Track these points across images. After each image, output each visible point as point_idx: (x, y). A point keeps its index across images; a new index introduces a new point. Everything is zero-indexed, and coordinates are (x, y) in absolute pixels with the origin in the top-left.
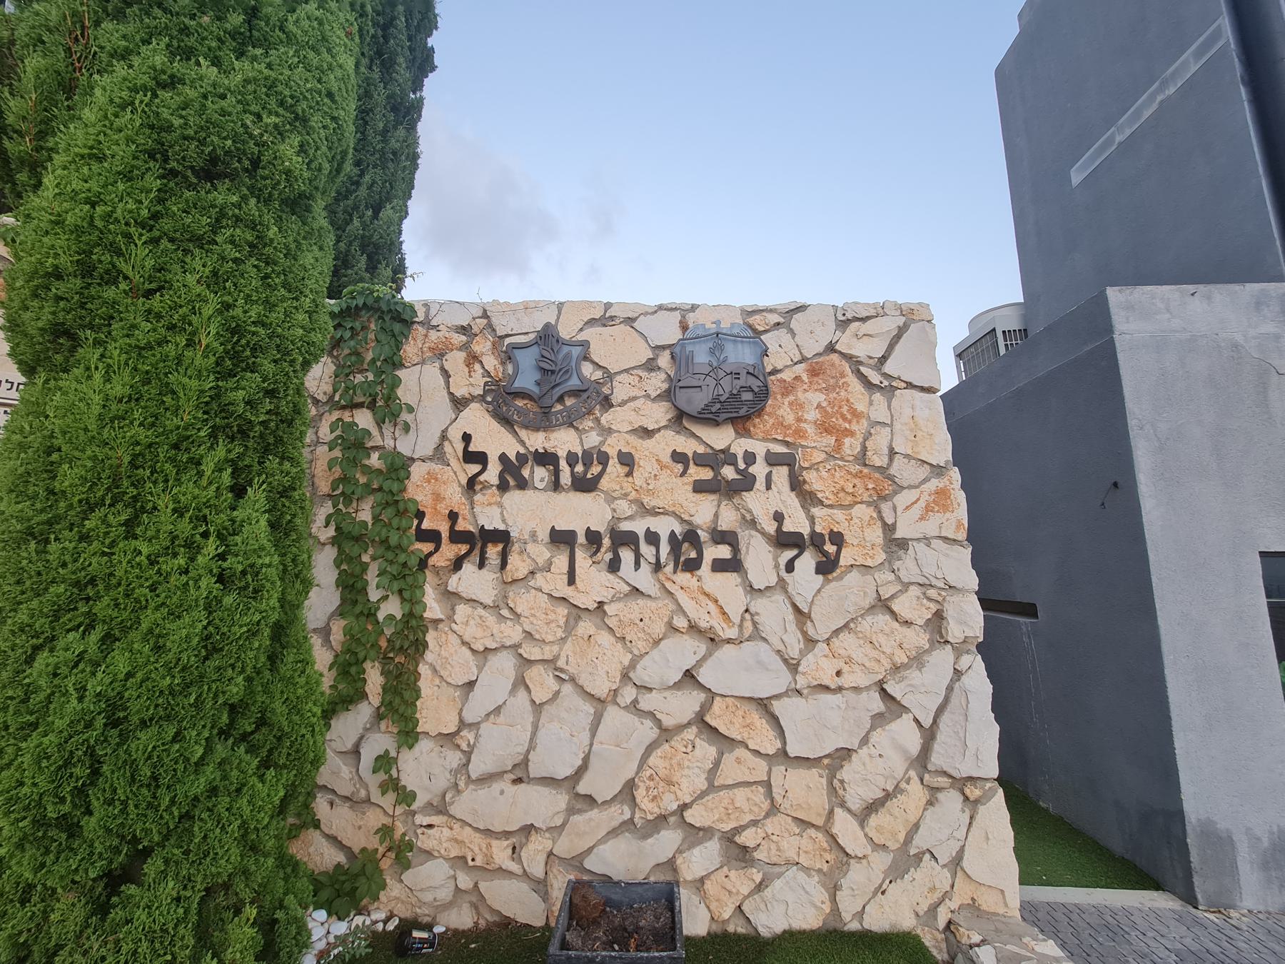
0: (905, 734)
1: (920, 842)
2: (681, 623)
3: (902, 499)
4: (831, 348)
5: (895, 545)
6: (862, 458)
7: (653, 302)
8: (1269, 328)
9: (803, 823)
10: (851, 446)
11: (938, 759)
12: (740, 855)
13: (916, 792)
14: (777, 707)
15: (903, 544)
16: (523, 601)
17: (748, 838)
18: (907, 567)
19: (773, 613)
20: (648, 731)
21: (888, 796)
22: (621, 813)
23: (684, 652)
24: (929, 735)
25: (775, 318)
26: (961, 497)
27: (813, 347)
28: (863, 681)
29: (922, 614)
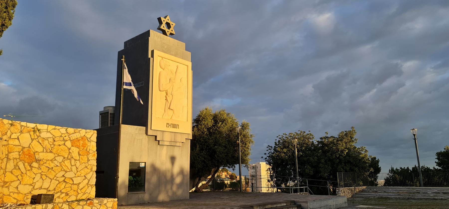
0: (86, 181)
2: (63, 169)
3: (90, 155)
5: (88, 160)
8: (137, 132)
9: (74, 191)
10: (85, 148)
13: (87, 187)
14: (73, 179)
16: (42, 167)
17: (68, 193)
18: (89, 163)
19: (74, 168)
20: (58, 182)
26: (96, 155)
27: (82, 135)
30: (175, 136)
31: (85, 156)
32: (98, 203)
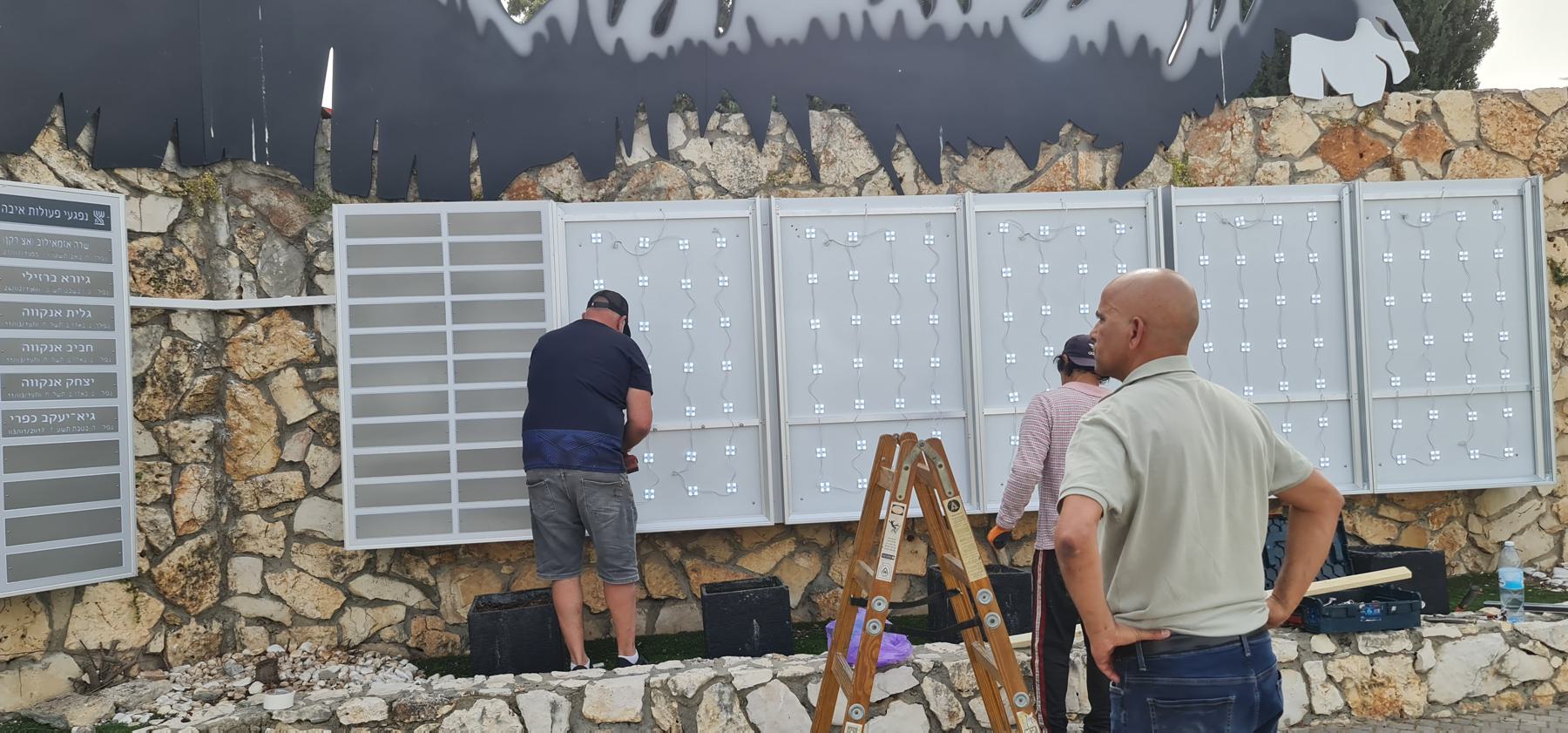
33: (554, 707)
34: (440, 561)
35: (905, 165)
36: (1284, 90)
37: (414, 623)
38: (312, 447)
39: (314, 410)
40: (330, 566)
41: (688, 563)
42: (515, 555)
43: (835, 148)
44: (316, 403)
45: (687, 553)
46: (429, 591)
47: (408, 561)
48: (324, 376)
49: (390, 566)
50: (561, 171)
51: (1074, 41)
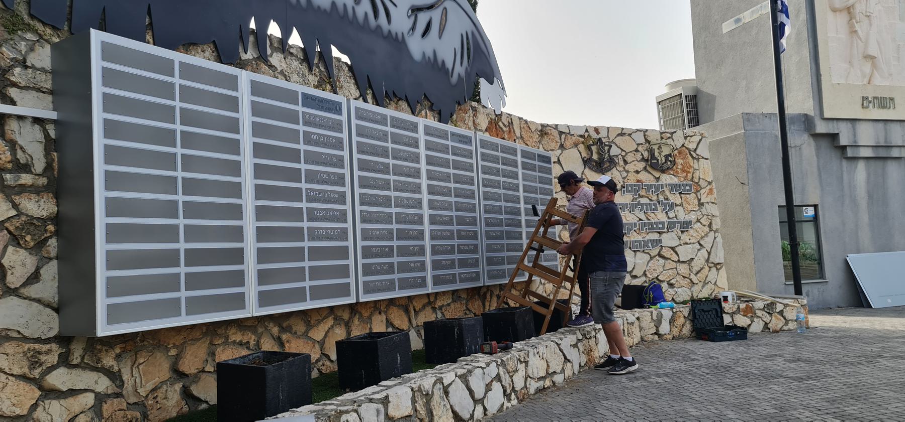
0: (704, 253)
1: (708, 279)
3: (702, 191)
4: (683, 146)
5: (701, 204)
6: (692, 180)
7: (634, 128)
10: (690, 175)
11: (711, 260)
12: (671, 285)
14: (677, 249)
15: (702, 204)
17: (673, 282)
21: (701, 269)
22: (644, 279)
23: (655, 236)
24: (709, 253)
25: (669, 135)
28: (695, 241)
29: (707, 223)
30: (886, 129)
31: (693, 195)
32: (763, 310)
33: (378, 411)
34: (124, 350)
35: (369, 98)
36: (479, 101)
37: (105, 406)
38: (10, 249)
39: (13, 213)
40: (26, 364)
41: (284, 337)
42: (179, 340)
43: (342, 79)
44: (15, 206)
45: (283, 330)
46: (114, 376)
47: (100, 351)
48: (22, 181)
49: (83, 358)
50: (203, 51)
51: (424, 54)
